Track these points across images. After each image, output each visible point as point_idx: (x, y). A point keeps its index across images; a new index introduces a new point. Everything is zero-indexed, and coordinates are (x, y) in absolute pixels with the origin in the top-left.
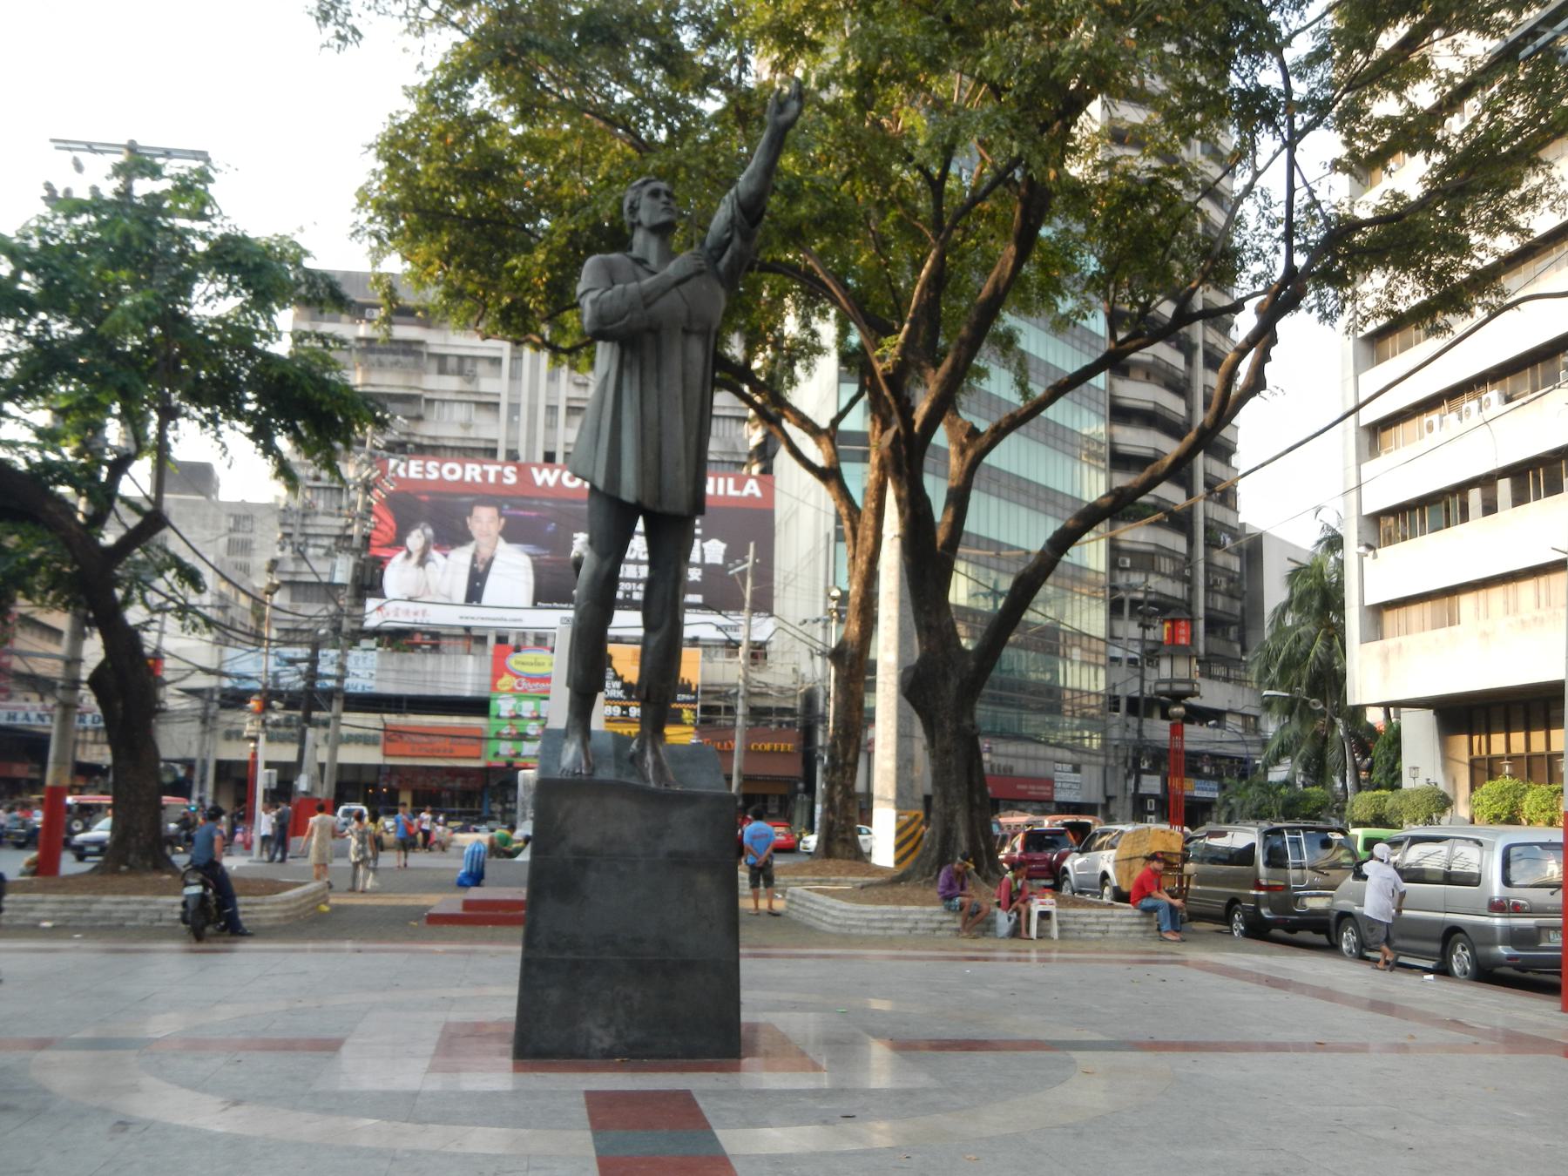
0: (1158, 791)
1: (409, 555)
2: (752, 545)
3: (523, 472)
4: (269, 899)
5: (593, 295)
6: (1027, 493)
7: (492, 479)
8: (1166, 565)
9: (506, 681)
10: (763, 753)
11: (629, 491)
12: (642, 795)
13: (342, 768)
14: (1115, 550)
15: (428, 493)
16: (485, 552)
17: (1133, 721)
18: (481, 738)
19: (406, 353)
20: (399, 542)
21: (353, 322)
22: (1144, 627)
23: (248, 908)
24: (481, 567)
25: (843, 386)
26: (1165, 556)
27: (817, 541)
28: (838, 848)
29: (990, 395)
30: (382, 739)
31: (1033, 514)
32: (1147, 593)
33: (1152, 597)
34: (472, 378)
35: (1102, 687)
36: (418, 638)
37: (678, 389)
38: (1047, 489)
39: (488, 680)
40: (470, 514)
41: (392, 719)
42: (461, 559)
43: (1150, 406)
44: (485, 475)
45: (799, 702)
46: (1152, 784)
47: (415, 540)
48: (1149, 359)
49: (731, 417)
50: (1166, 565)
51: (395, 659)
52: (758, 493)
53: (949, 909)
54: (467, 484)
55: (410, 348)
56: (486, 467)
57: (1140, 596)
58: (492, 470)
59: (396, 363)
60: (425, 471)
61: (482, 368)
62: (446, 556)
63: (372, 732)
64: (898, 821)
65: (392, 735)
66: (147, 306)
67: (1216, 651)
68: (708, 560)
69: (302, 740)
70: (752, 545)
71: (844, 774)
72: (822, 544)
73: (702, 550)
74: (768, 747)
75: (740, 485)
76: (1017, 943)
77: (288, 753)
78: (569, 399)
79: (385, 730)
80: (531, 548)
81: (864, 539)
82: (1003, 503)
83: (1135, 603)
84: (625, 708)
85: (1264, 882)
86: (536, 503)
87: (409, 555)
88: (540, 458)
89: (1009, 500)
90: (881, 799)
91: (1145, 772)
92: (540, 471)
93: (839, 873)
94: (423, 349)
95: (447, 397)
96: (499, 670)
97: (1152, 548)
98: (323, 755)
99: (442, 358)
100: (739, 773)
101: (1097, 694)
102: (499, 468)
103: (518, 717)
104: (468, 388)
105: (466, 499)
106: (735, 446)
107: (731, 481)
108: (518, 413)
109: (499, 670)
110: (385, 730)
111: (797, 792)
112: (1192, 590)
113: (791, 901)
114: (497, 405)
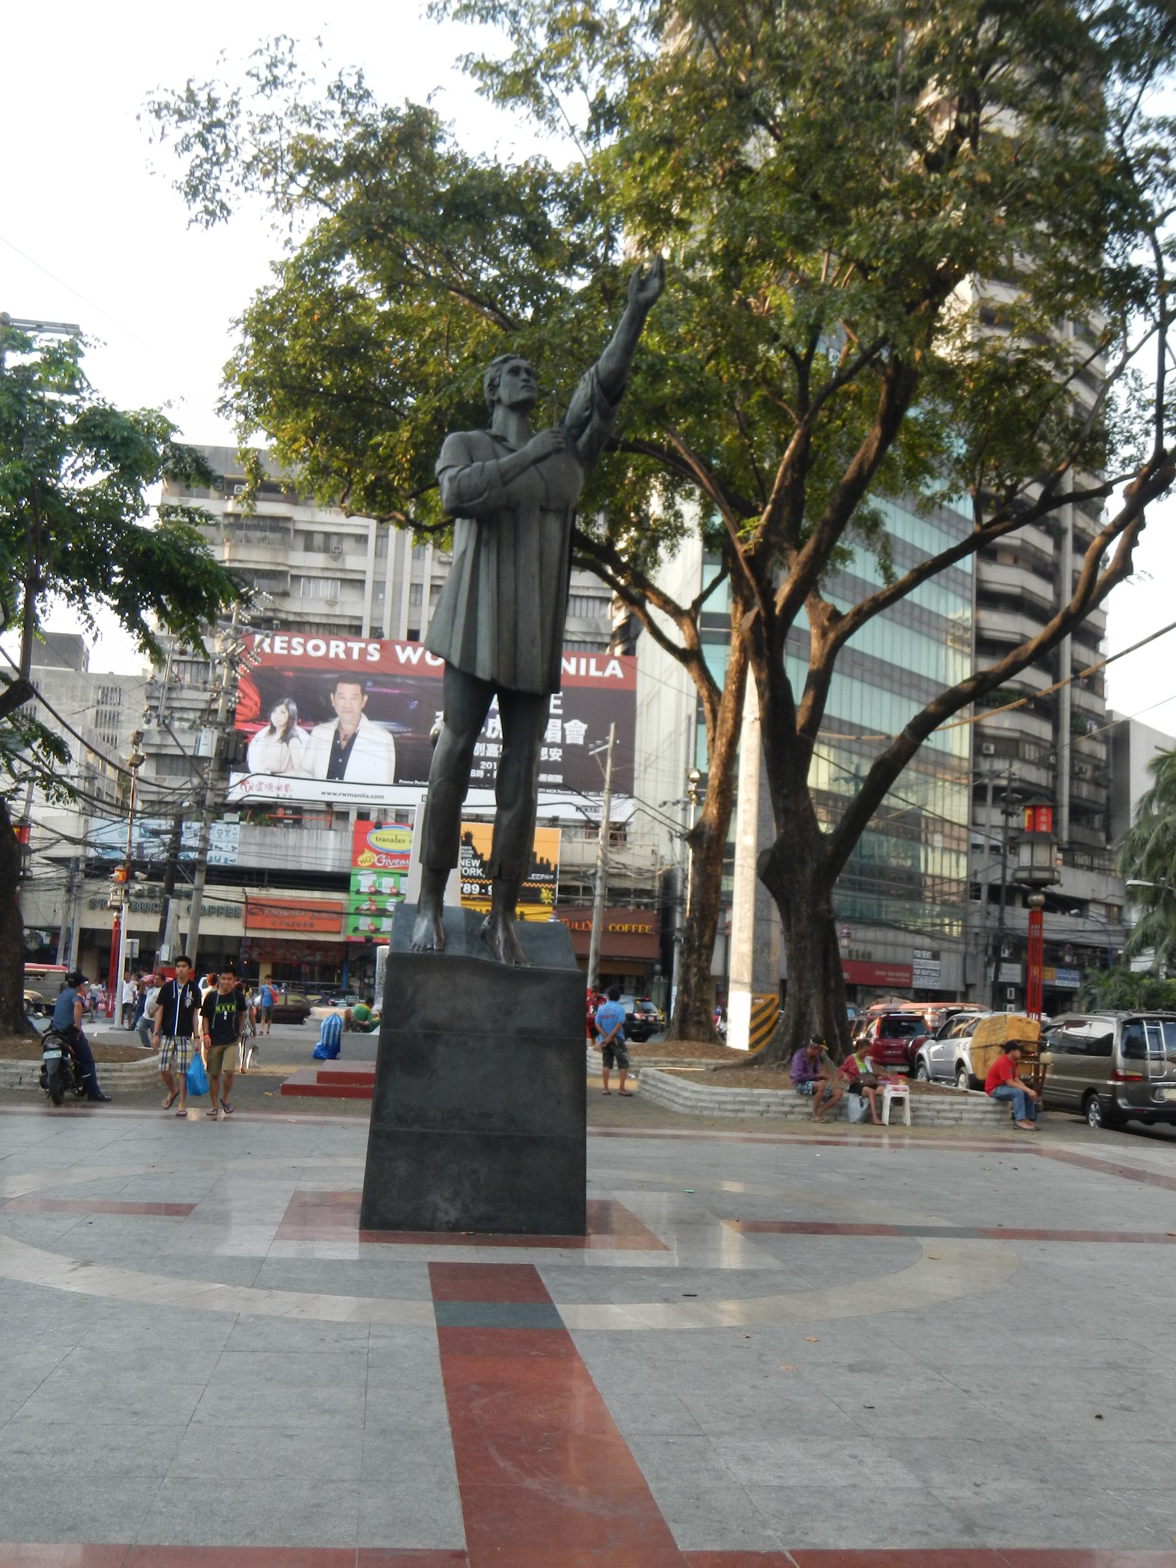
0: (1018, 979)
1: (273, 730)
2: (613, 726)
3: (387, 649)
4: (126, 1065)
5: (451, 472)
6: (891, 678)
7: (355, 656)
8: (1031, 752)
9: (367, 857)
10: (621, 933)
11: (484, 669)
12: (492, 971)
13: (203, 938)
14: (979, 736)
15: (291, 670)
16: (348, 729)
17: (994, 909)
18: (341, 914)
19: (273, 529)
20: (263, 718)
21: (221, 498)
22: (1007, 813)
23: (105, 1073)
24: (344, 744)
25: (707, 567)
26: (1029, 743)
27: (678, 723)
28: (692, 1030)
29: (855, 578)
30: (243, 912)
31: (897, 698)
32: (1010, 779)
33: (1016, 785)
34: (337, 555)
35: (963, 874)
36: (280, 813)
37: (535, 568)
38: (911, 673)
39: (349, 856)
40: (334, 691)
41: (253, 892)
42: (324, 733)
43: (1018, 591)
44: (348, 651)
45: (657, 884)
46: (1012, 973)
47: (279, 715)
48: (1017, 543)
49: (594, 598)
50: (1031, 752)
51: (257, 834)
52: (620, 675)
53: (801, 1093)
54: (331, 661)
55: (277, 524)
56: (350, 644)
57: (1004, 783)
58: (356, 646)
59: (264, 539)
60: (290, 647)
61: (348, 545)
62: (309, 732)
63: (234, 905)
64: (753, 1004)
65: (253, 908)
66: (16, 478)
67: (1080, 839)
68: (568, 741)
69: (165, 912)
70: (613, 726)
71: (700, 956)
72: (684, 726)
73: (563, 730)
74: (625, 928)
75: (601, 666)
76: (868, 1128)
77: (151, 924)
78: (433, 578)
79: (246, 903)
80: (393, 726)
81: (723, 721)
82: (866, 687)
83: (998, 790)
84: (482, 886)
85: (1121, 1073)
86: (399, 680)
87: (273, 730)
88: (403, 636)
89: (872, 684)
90: (736, 982)
91: (1005, 960)
92: (403, 650)
93: (692, 1054)
94: (290, 526)
95: (313, 574)
96: (360, 845)
97: (1017, 735)
98: (184, 926)
99: (309, 534)
100: (596, 954)
101: (958, 881)
102: (363, 645)
103: (378, 893)
104: (333, 565)
105: (329, 676)
106: (598, 626)
107: (593, 662)
108: (383, 591)
109: (360, 845)
110: (246, 903)
111: (654, 974)
112: (1056, 777)
113: (643, 1082)
114: (363, 582)
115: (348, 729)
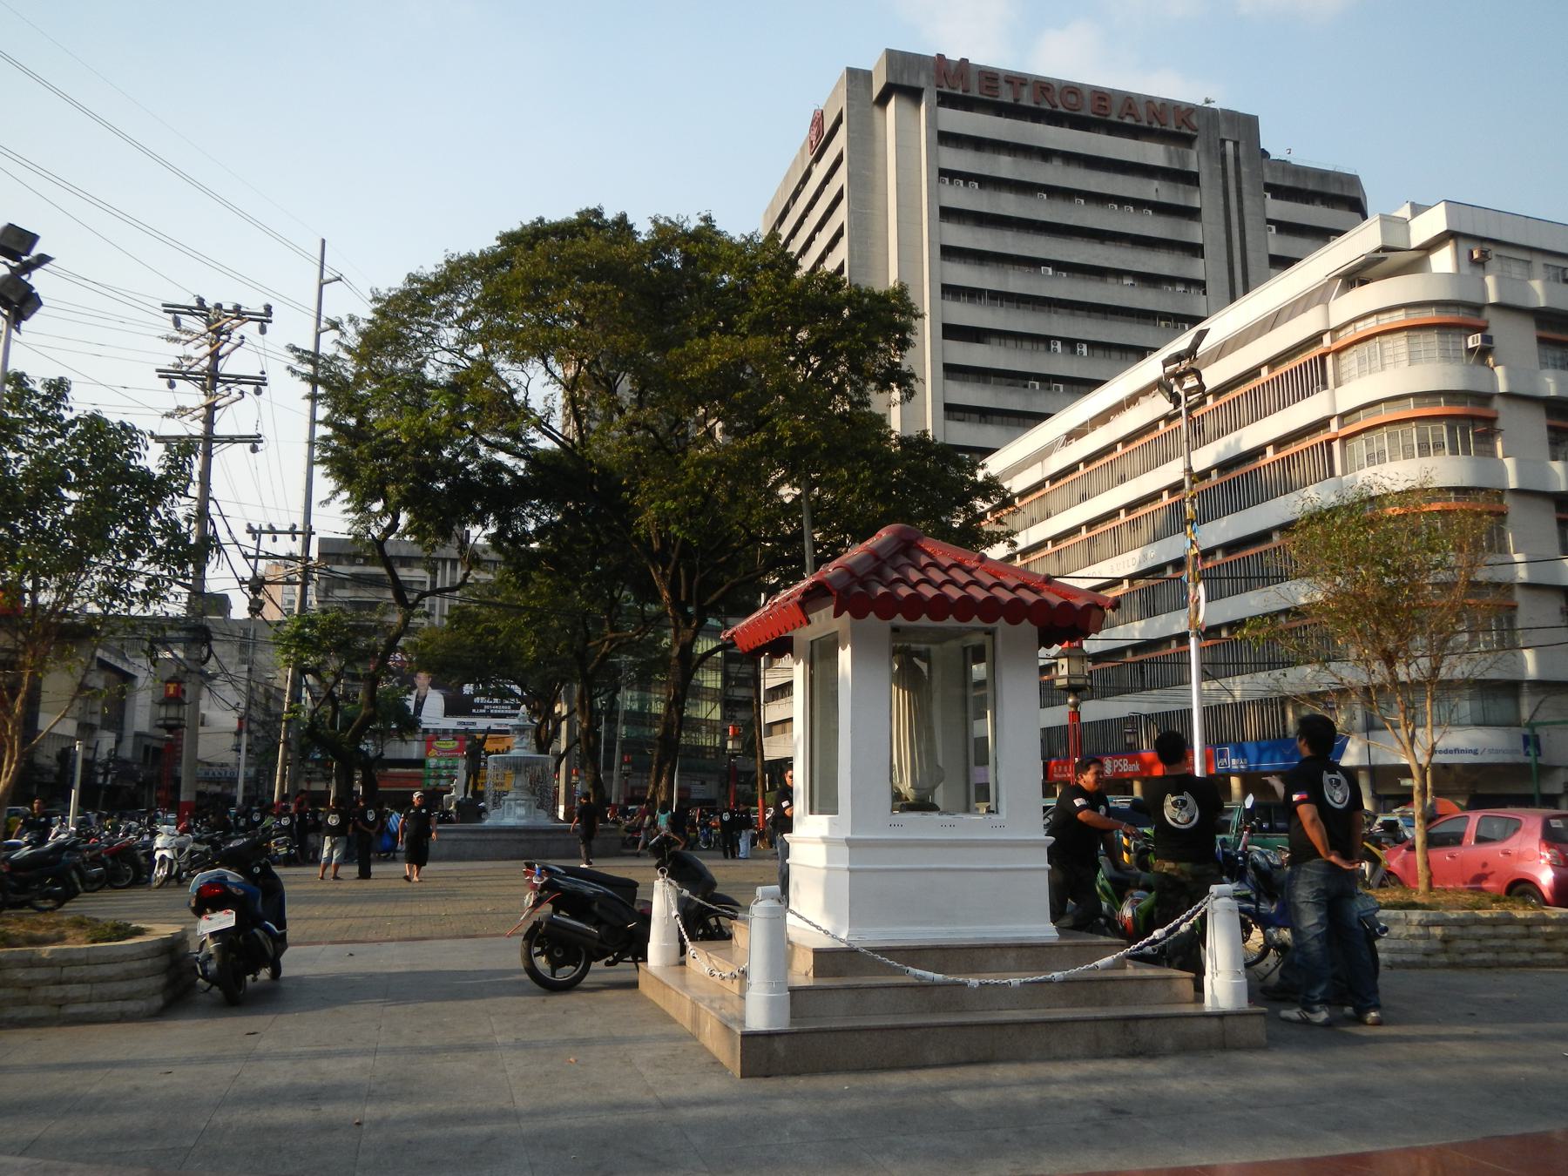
9: (433, 752)
16: (422, 694)
39: (424, 750)
103: (438, 768)
109: (429, 748)
115: (422, 694)
